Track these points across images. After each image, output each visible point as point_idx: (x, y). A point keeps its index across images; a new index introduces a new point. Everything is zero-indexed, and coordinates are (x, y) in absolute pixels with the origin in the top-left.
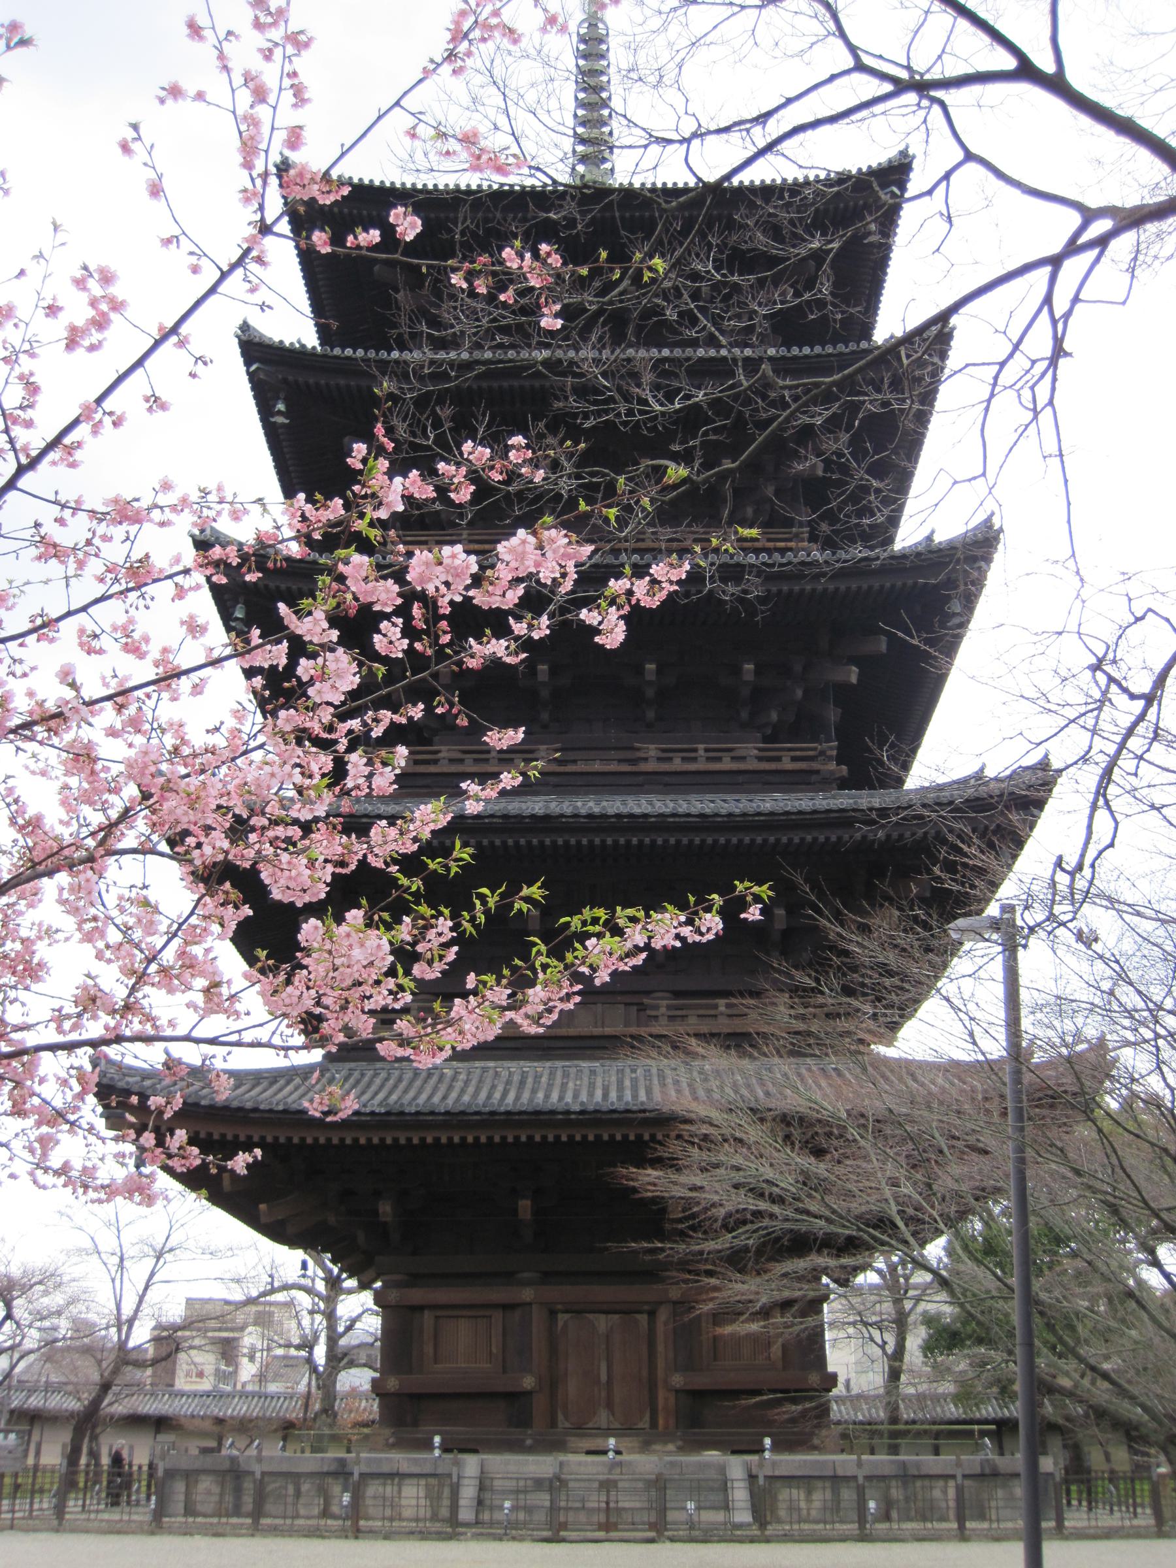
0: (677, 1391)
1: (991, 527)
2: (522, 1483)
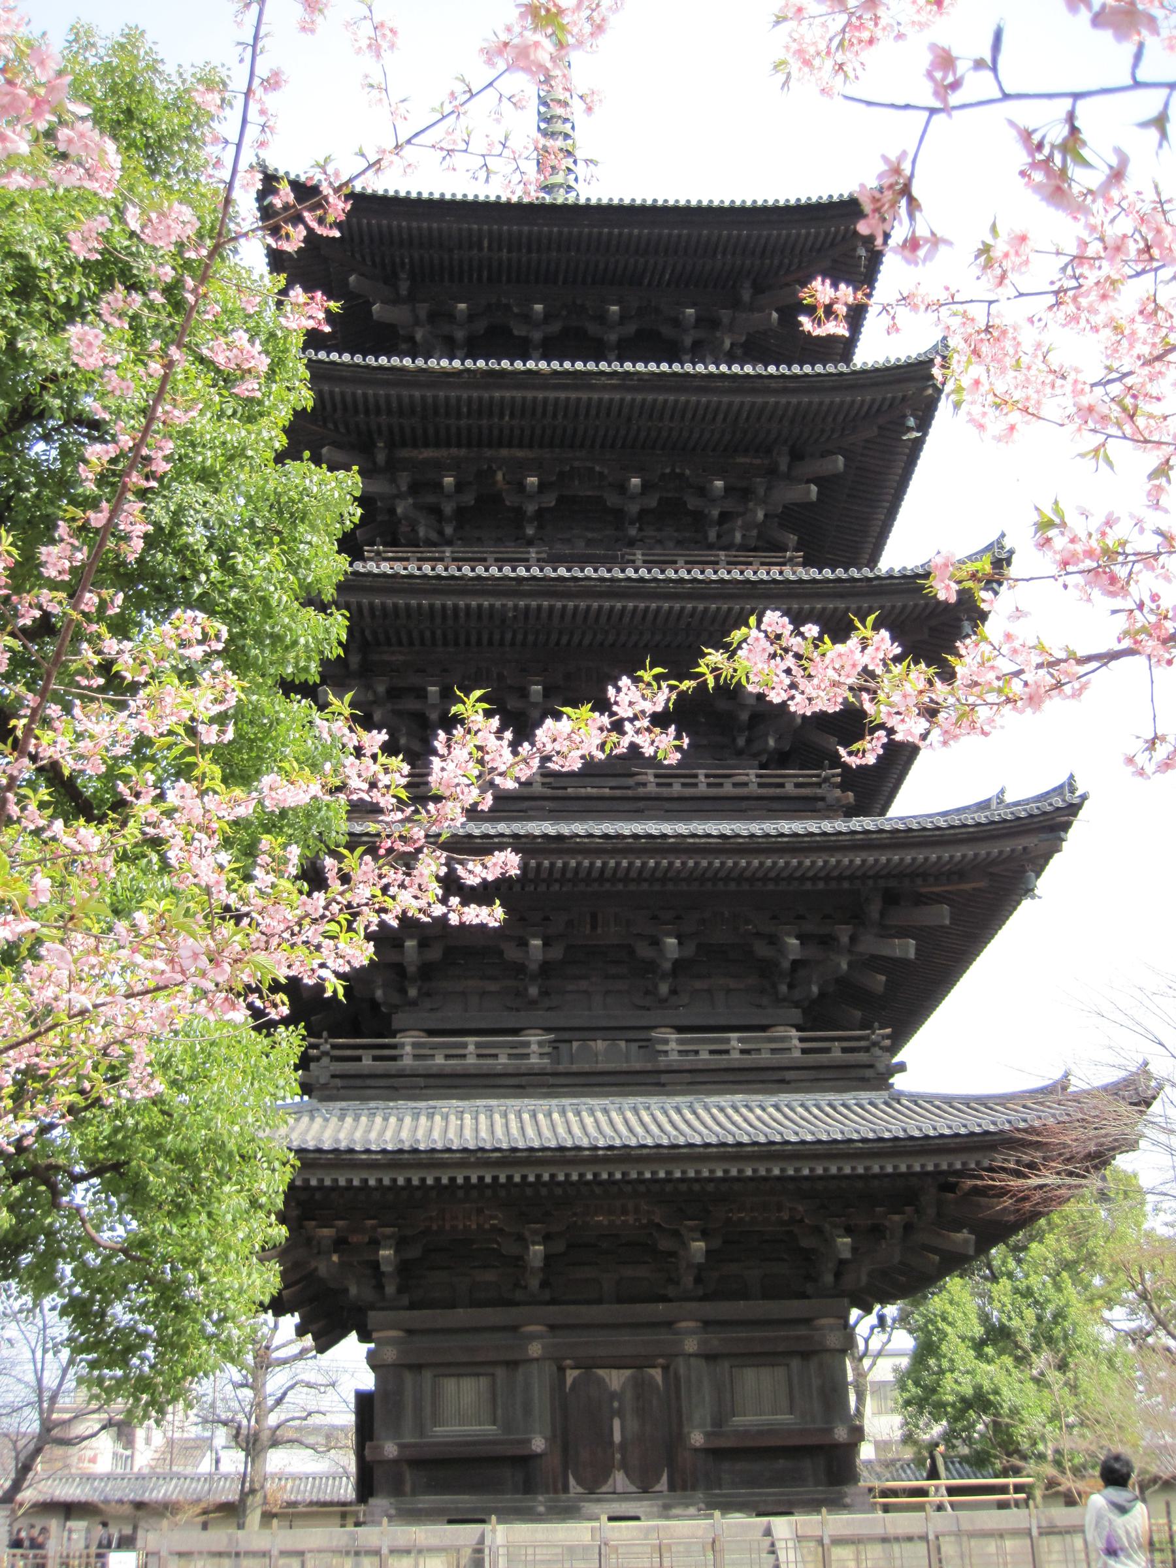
0: (696, 1450)
1: (1002, 548)
2: (559, 1550)
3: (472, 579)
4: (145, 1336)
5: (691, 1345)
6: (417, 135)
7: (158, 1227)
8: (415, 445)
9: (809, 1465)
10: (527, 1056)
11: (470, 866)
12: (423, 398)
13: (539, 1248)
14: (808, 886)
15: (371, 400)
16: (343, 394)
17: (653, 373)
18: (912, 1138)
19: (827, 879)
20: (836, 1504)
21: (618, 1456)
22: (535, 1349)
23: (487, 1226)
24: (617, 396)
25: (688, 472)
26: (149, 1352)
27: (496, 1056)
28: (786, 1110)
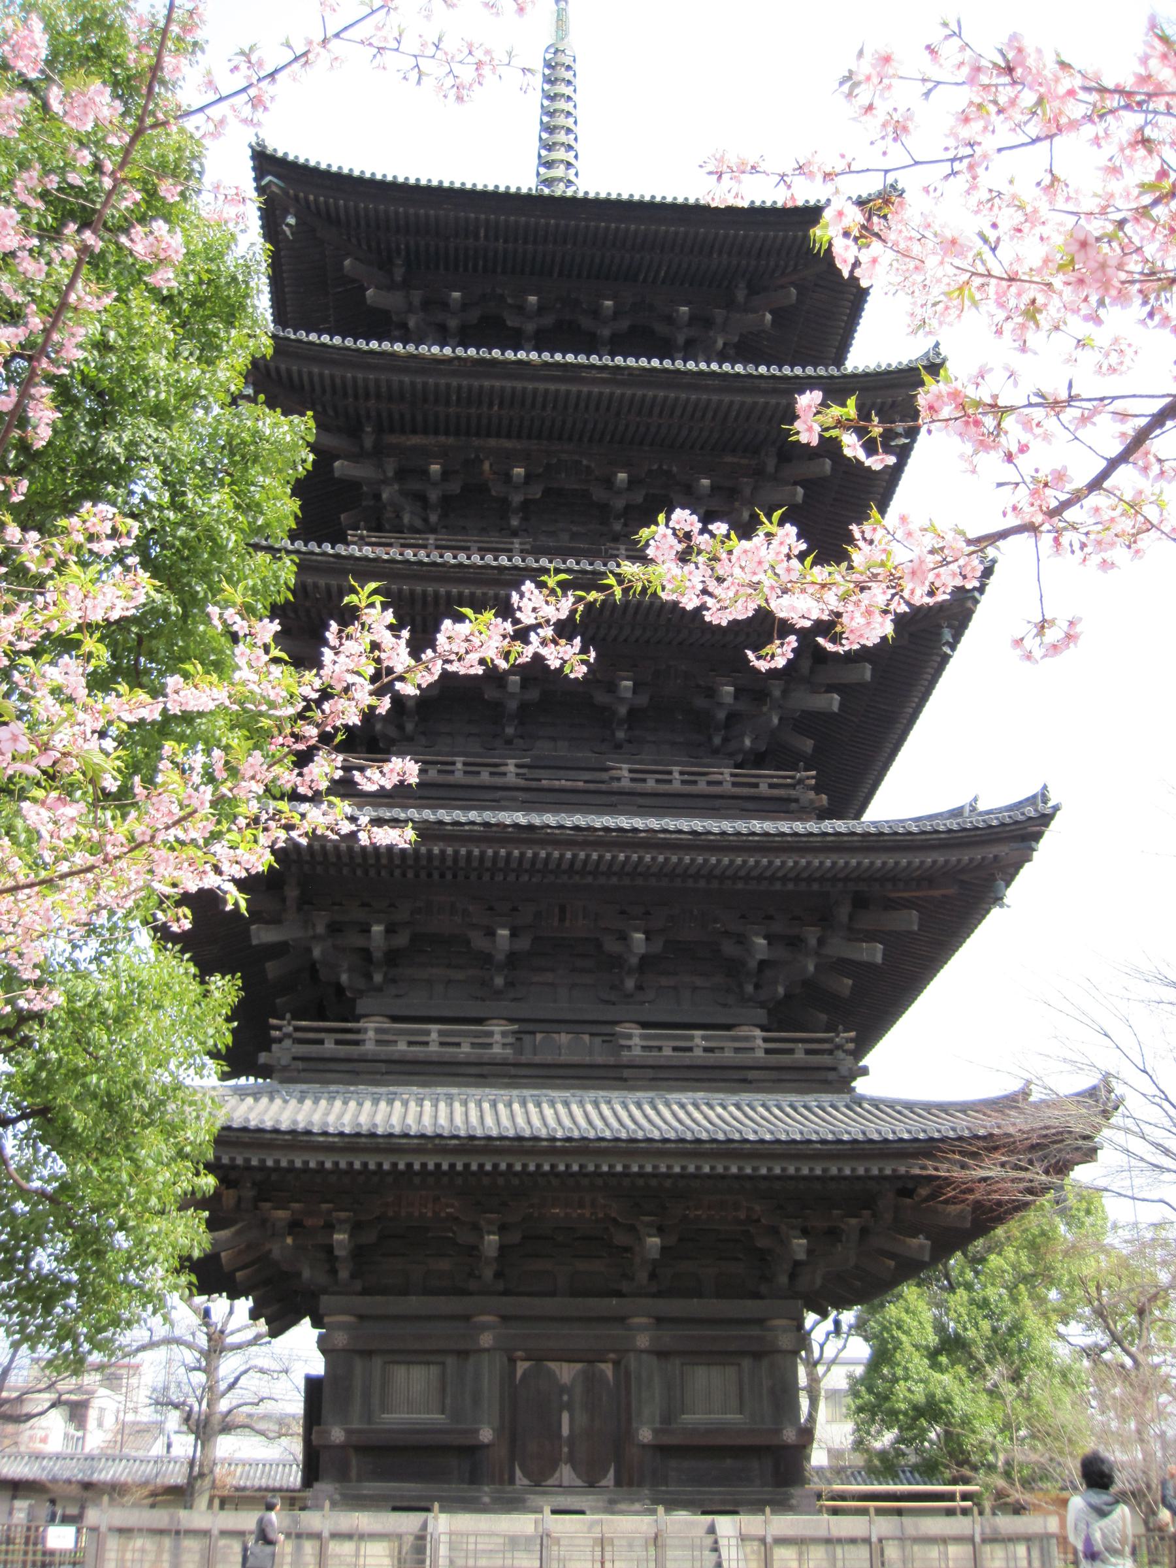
0: (644, 1446)
3: (454, 566)
4: (68, 1285)
5: (643, 1341)
6: (346, 29)
7: (80, 1168)
8: (403, 431)
9: (758, 1465)
10: (490, 1045)
11: (368, 773)
12: (413, 384)
13: (494, 1238)
14: (778, 886)
15: (360, 383)
16: (332, 378)
17: (644, 369)
18: (871, 1141)
19: (797, 879)
20: (782, 1505)
21: (565, 1450)
22: (486, 1340)
23: (443, 1215)
24: (607, 391)
25: (675, 469)
26: (72, 1301)
27: (458, 1045)
28: (747, 1109)
